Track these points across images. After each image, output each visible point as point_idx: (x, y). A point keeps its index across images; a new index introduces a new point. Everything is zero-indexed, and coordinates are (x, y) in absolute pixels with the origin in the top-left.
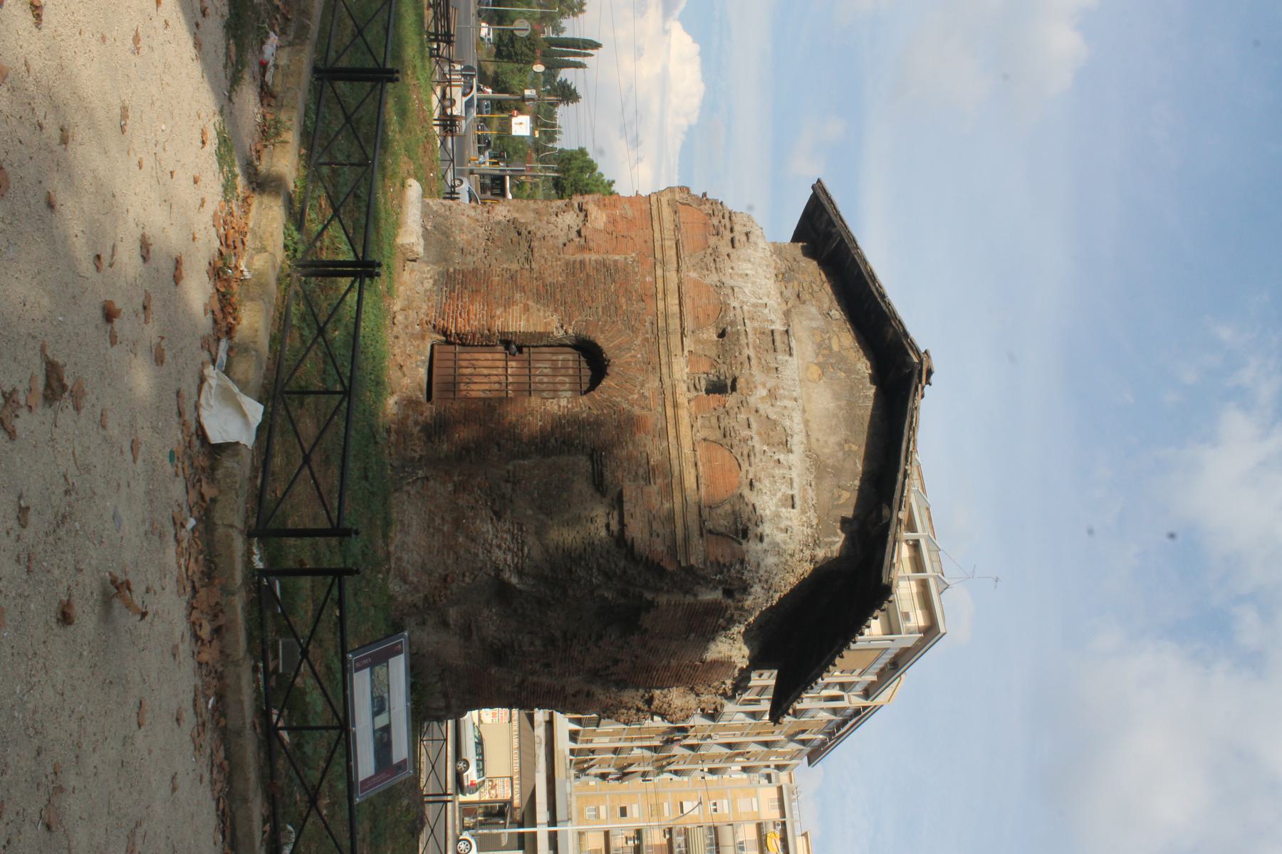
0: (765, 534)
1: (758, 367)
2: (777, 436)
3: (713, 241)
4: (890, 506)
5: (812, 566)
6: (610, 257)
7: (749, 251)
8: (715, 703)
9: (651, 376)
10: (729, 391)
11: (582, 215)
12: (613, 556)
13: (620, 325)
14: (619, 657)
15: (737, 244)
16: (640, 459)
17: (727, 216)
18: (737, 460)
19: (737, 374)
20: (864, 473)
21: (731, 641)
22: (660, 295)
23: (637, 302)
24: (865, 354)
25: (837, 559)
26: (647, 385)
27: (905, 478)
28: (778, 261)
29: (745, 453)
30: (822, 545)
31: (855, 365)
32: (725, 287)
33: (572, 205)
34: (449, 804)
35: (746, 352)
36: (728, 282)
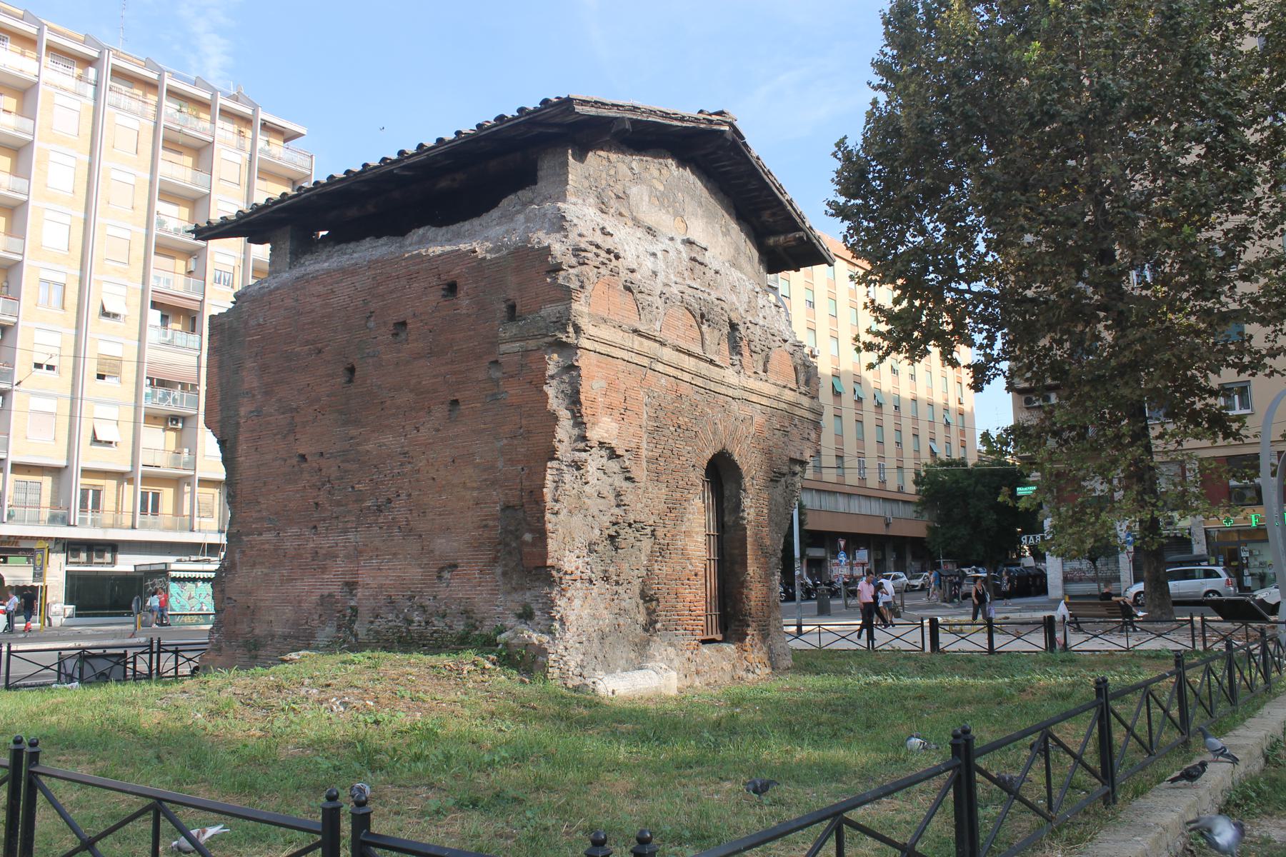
24: (664, 158)
34: (13, 648)
36: (659, 288)
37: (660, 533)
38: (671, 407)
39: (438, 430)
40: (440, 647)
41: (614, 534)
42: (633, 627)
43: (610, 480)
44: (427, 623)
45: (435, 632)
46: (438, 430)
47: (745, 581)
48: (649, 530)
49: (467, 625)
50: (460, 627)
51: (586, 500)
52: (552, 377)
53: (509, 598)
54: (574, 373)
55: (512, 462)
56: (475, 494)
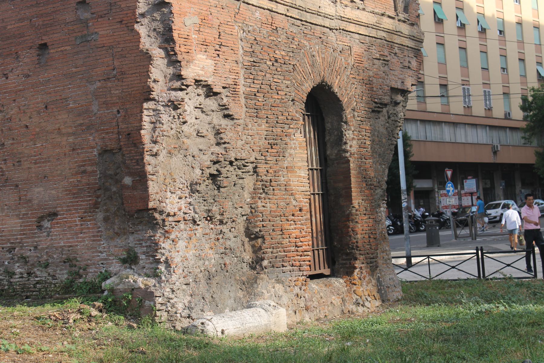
26: (336, 45)
37: (262, 169)
38: (267, 41)
39: (28, 76)
40: (44, 298)
41: (215, 173)
42: (239, 266)
43: (209, 119)
44: (29, 274)
45: (38, 282)
46: (28, 76)
47: (350, 214)
48: (250, 167)
49: (70, 273)
50: (63, 276)
51: (185, 140)
52: (143, 15)
53: (112, 243)
54: (165, 10)
55: (107, 104)
56: (71, 139)
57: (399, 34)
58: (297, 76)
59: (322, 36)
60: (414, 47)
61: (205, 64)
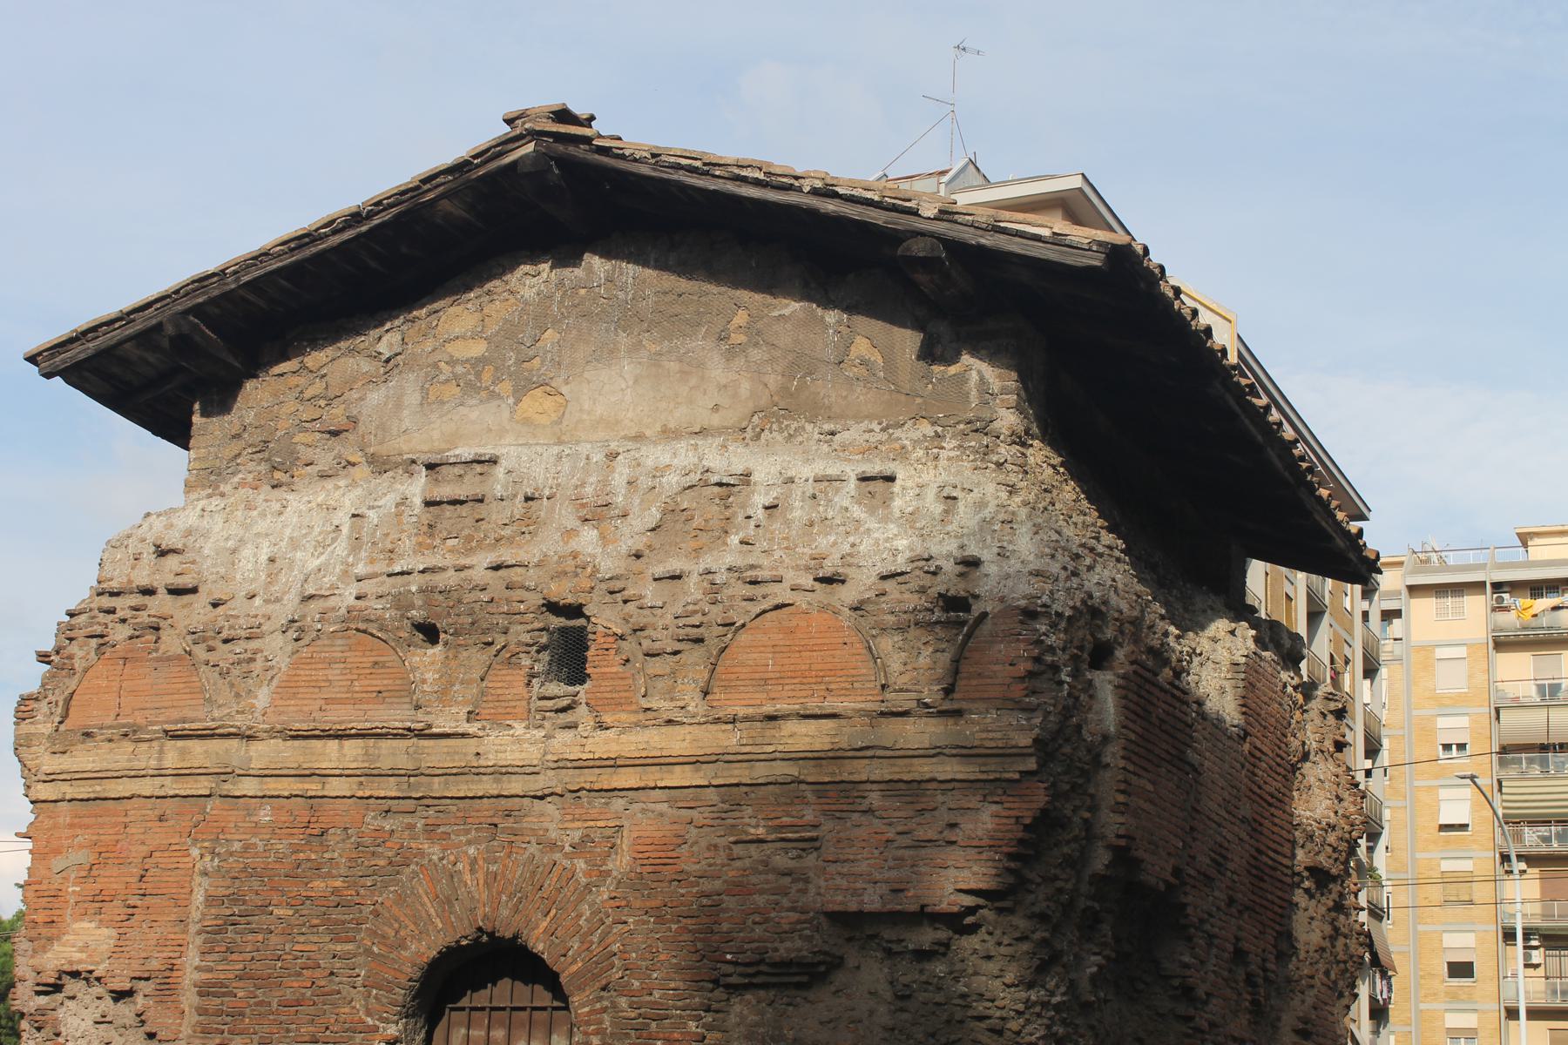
0: (958, 554)
1: (520, 546)
2: (707, 510)
3: (172, 643)
4: (895, 238)
5: (1036, 443)
6: (196, 915)
7: (206, 552)
8: (1324, 715)
9: (529, 822)
10: (581, 622)
11: (72, 986)
12: (999, 944)
13: (387, 897)
14: (1230, 948)
15: (186, 581)
16: (747, 862)
17: (107, 602)
18: (764, 612)
19: (535, 600)
20: (806, 296)
21: (1196, 660)
22: (313, 787)
23: (327, 849)
24: (499, 275)
25: (1023, 379)
26: (553, 835)
27: (836, 195)
28: (236, 479)
29: (749, 590)
30: (987, 415)
31: (526, 303)
32: (304, 617)
33: (41, 1011)
35: (479, 574)
36: (289, 606)
57: (869, 753)
58: (386, 928)
59: (495, 820)
60: (972, 777)
61: (92, 938)
